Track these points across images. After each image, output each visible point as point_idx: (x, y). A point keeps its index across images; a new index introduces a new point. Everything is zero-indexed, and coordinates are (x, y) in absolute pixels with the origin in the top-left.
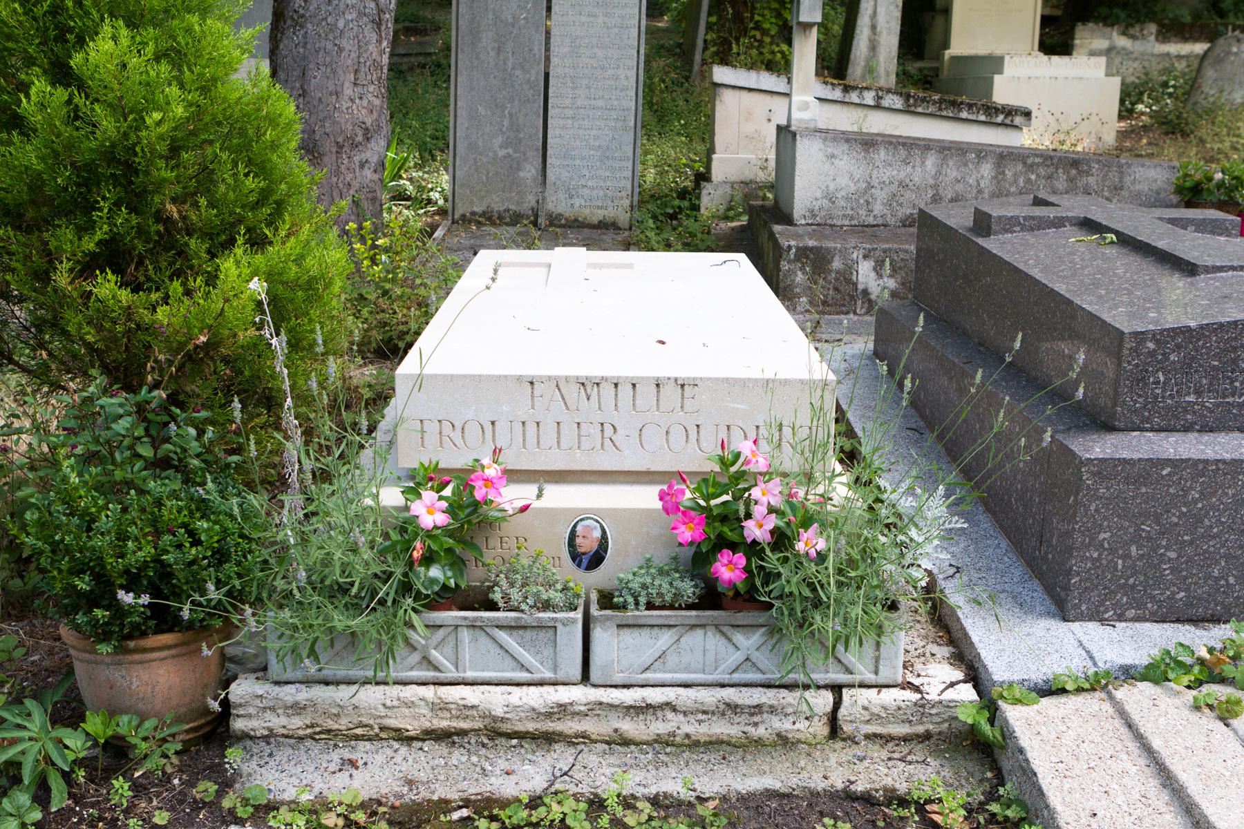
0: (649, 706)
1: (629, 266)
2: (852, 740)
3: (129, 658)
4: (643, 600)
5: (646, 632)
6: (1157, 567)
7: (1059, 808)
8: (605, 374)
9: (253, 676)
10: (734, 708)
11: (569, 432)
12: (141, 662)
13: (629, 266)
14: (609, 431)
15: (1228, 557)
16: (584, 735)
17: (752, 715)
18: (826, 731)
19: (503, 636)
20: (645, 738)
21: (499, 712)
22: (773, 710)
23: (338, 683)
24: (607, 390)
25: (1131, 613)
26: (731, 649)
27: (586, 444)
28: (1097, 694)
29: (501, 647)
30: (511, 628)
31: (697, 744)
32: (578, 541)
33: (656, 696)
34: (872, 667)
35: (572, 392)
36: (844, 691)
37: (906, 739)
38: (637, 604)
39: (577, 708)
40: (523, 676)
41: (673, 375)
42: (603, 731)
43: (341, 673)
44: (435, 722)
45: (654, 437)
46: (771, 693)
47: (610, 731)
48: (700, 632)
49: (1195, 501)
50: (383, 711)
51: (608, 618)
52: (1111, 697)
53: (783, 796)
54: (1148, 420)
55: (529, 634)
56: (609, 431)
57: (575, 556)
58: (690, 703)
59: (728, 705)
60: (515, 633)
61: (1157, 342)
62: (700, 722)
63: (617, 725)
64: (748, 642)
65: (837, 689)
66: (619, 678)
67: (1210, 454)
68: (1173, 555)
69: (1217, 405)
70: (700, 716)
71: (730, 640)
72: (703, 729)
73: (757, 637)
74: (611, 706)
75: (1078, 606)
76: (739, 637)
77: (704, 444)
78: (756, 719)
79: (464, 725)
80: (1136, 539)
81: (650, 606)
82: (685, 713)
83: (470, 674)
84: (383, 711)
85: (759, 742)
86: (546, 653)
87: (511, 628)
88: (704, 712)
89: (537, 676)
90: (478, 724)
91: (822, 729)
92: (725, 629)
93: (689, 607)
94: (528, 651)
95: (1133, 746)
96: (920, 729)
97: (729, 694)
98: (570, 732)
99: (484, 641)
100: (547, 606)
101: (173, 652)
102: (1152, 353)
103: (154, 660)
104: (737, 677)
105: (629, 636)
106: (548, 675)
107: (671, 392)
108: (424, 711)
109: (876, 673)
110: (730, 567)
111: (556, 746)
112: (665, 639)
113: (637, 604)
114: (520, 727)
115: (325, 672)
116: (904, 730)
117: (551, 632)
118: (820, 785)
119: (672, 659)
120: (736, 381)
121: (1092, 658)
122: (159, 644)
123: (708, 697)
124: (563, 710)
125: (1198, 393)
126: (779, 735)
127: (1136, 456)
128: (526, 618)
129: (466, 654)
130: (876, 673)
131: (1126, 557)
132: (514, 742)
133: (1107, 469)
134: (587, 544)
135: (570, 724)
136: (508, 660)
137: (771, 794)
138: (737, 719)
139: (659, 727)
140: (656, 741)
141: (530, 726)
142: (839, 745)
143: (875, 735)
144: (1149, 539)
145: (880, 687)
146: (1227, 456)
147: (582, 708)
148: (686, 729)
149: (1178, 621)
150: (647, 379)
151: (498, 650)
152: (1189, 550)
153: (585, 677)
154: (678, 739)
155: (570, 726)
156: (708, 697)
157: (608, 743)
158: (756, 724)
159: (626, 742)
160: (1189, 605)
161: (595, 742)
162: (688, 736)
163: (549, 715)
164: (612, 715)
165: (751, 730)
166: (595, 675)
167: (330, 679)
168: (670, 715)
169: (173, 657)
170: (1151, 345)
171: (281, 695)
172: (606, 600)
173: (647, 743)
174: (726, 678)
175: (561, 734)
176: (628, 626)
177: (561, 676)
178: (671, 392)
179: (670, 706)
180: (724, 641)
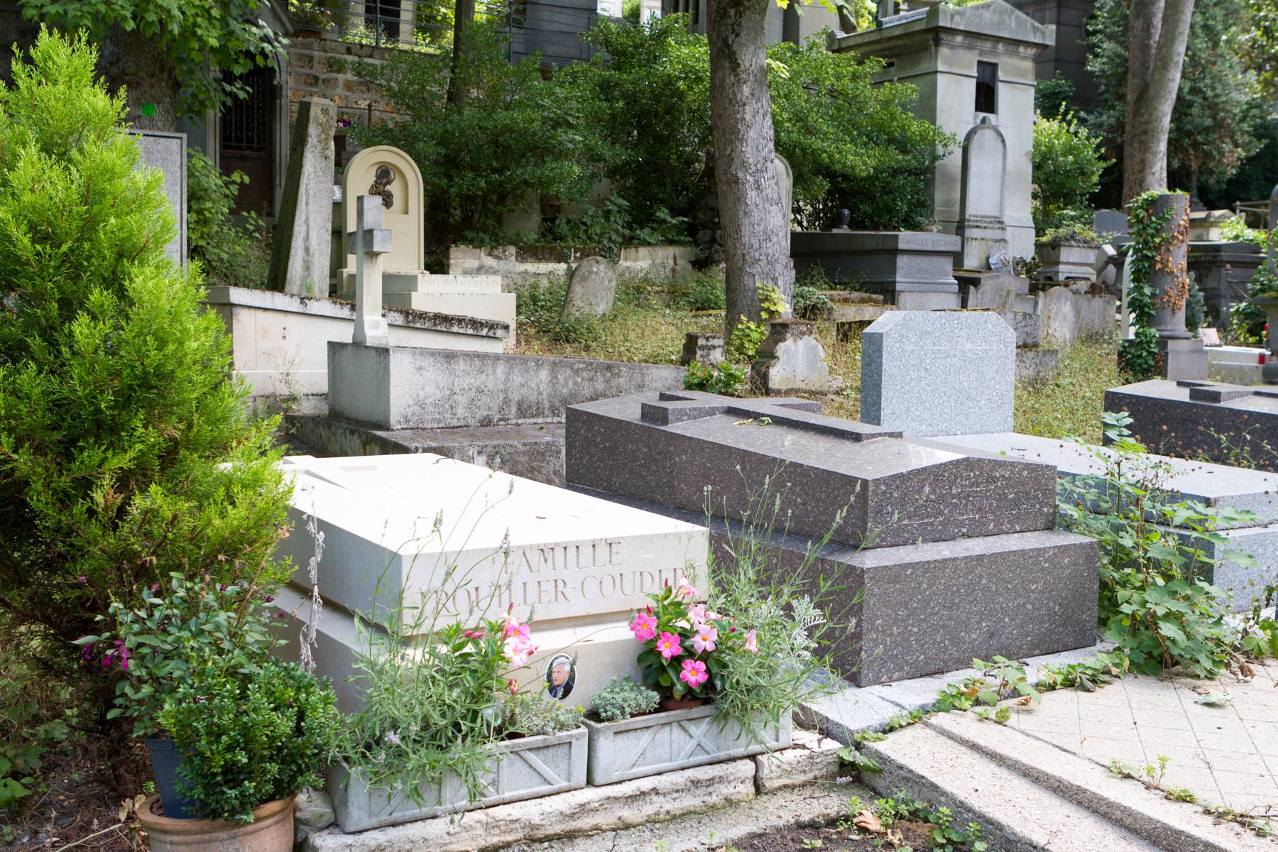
0: (643, 793)
1: (373, 468)
2: (774, 792)
3: (243, 830)
4: (628, 710)
5: (632, 734)
6: (907, 640)
7: (955, 791)
8: (558, 541)
9: (327, 831)
10: (696, 783)
11: (532, 590)
12: (253, 832)
13: (373, 468)
14: (560, 584)
15: (945, 627)
16: (597, 828)
17: (708, 786)
18: (753, 790)
19: (531, 756)
20: (640, 820)
21: (537, 821)
22: (721, 780)
23: (403, 823)
24: (559, 552)
25: (896, 675)
26: (688, 738)
27: (545, 598)
28: (917, 725)
29: (531, 766)
30: (539, 749)
31: (674, 817)
32: (554, 676)
33: (646, 784)
34: (773, 737)
35: (535, 557)
36: (759, 757)
37: (803, 785)
38: (623, 713)
39: (592, 805)
40: (546, 788)
41: (604, 537)
42: (610, 821)
43: (409, 814)
44: (489, 839)
45: (592, 587)
46: (717, 767)
47: (615, 820)
48: (667, 728)
49: (925, 590)
50: (447, 839)
51: (608, 728)
52: (927, 725)
53: (760, 836)
54: (883, 540)
55: (551, 752)
56: (560, 584)
57: (553, 690)
58: (668, 786)
59: (692, 782)
60: (541, 752)
61: (886, 485)
62: (674, 799)
63: (620, 814)
64: (700, 730)
65: (753, 757)
66: (615, 778)
67: (928, 557)
68: (915, 630)
69: (920, 525)
70: (675, 795)
71: (686, 731)
72: (678, 805)
73: (704, 725)
74: (616, 798)
75: (866, 676)
76: (692, 728)
77: (625, 589)
78: (710, 789)
79: (509, 838)
80: (896, 621)
81: (632, 715)
82: (664, 795)
83: (508, 795)
84: (447, 839)
85: (713, 807)
86: (562, 766)
87: (539, 749)
88: (677, 791)
89: (556, 787)
90: (520, 835)
91: (749, 788)
92: (684, 723)
93: (656, 711)
94: (549, 766)
95: (964, 749)
96: (810, 776)
97: (690, 773)
98: (586, 827)
99: (519, 764)
100: (562, 727)
101: (276, 819)
102: (884, 493)
103: (262, 829)
104: (694, 760)
105: (621, 739)
106: (564, 784)
107: (602, 550)
108: (481, 831)
109: (777, 740)
110: (676, 680)
111: (578, 841)
112: (646, 737)
113: (623, 713)
114: (551, 831)
115: (394, 815)
116: (801, 778)
117: (567, 747)
118: (781, 823)
119: (650, 754)
120: (645, 537)
121: (897, 705)
122: (269, 812)
123: (680, 778)
124: (583, 809)
125: (910, 518)
126: (726, 799)
127: (891, 563)
128: (551, 739)
129: (505, 778)
130: (777, 740)
131: (892, 635)
132: (546, 844)
133: (897, 574)
134: (560, 678)
135: (586, 820)
136: (536, 777)
137: (753, 836)
138: (698, 792)
139: (648, 809)
140: (647, 821)
141: (558, 829)
142: (765, 798)
143: (785, 786)
144: (903, 620)
145: (781, 750)
146: (938, 557)
147: (597, 805)
148: (667, 807)
149: (921, 676)
150: (586, 541)
151: (528, 770)
152: (924, 625)
153: (590, 782)
154: (662, 816)
155: (586, 822)
156: (680, 778)
157: (614, 830)
158: (710, 793)
159: (627, 827)
160: (926, 664)
161: (604, 831)
162: (668, 812)
163: (572, 816)
164: (616, 806)
165: (707, 798)
166: (599, 777)
167: (400, 820)
168: (655, 798)
169: (276, 823)
170: (883, 488)
171: (367, 841)
172: (594, 715)
173: (642, 824)
174: (685, 762)
175: (580, 831)
176: (620, 732)
177: (573, 784)
178: (602, 550)
179: (655, 791)
180: (683, 733)
